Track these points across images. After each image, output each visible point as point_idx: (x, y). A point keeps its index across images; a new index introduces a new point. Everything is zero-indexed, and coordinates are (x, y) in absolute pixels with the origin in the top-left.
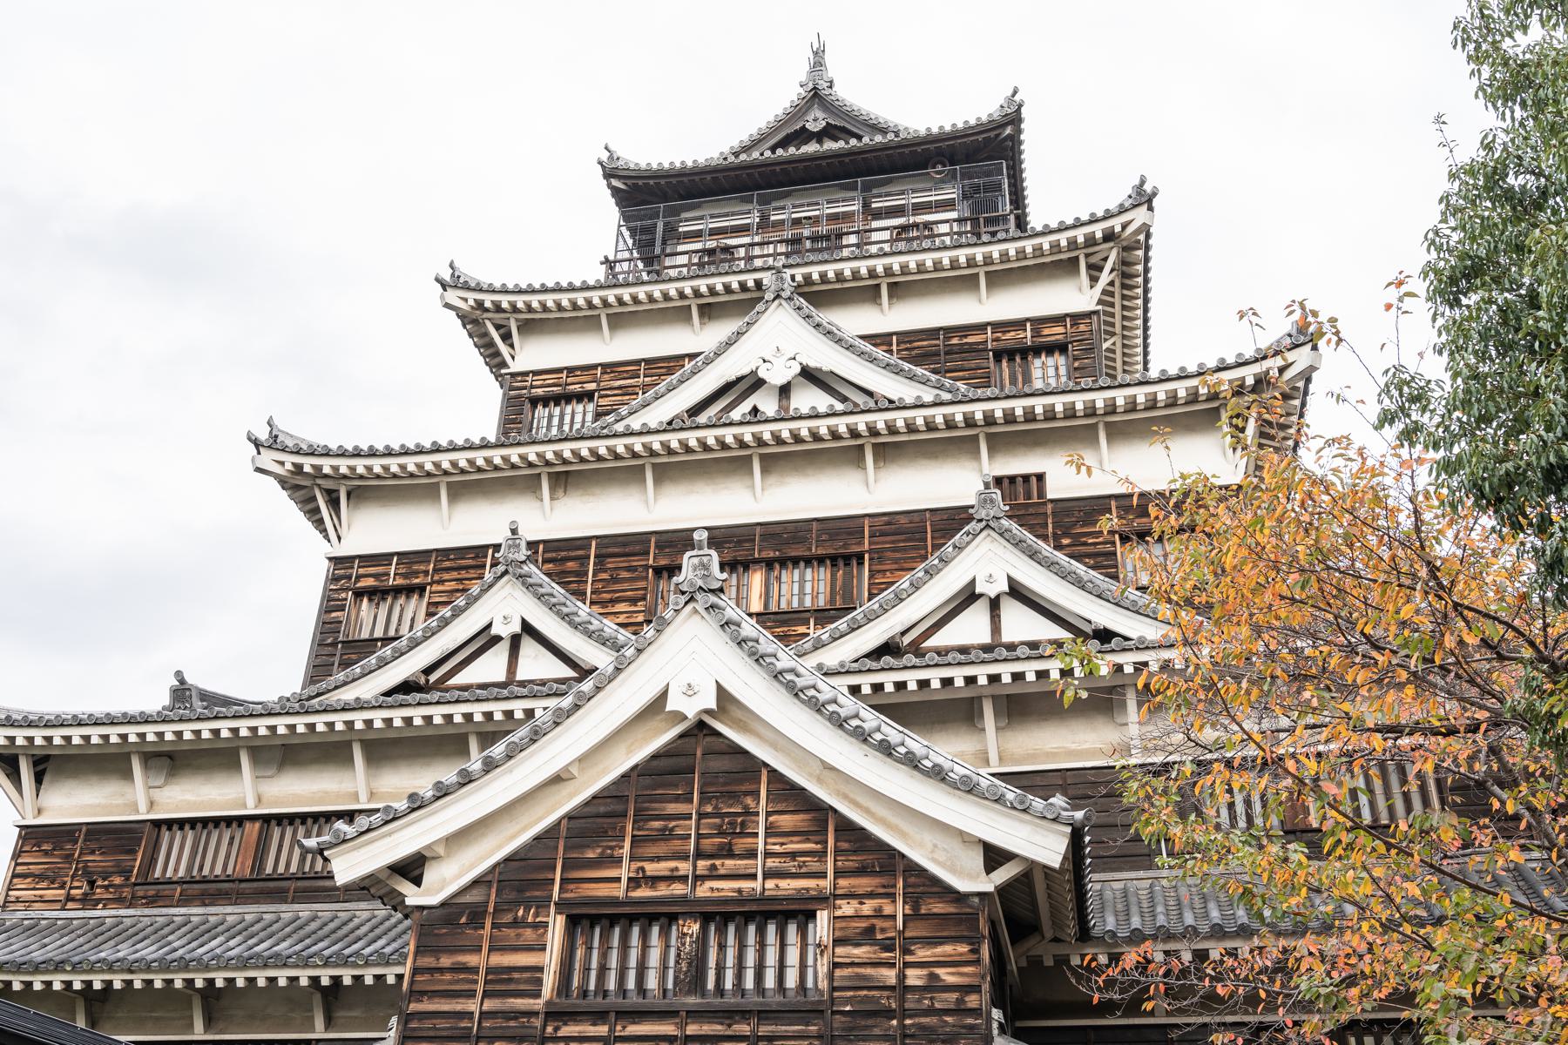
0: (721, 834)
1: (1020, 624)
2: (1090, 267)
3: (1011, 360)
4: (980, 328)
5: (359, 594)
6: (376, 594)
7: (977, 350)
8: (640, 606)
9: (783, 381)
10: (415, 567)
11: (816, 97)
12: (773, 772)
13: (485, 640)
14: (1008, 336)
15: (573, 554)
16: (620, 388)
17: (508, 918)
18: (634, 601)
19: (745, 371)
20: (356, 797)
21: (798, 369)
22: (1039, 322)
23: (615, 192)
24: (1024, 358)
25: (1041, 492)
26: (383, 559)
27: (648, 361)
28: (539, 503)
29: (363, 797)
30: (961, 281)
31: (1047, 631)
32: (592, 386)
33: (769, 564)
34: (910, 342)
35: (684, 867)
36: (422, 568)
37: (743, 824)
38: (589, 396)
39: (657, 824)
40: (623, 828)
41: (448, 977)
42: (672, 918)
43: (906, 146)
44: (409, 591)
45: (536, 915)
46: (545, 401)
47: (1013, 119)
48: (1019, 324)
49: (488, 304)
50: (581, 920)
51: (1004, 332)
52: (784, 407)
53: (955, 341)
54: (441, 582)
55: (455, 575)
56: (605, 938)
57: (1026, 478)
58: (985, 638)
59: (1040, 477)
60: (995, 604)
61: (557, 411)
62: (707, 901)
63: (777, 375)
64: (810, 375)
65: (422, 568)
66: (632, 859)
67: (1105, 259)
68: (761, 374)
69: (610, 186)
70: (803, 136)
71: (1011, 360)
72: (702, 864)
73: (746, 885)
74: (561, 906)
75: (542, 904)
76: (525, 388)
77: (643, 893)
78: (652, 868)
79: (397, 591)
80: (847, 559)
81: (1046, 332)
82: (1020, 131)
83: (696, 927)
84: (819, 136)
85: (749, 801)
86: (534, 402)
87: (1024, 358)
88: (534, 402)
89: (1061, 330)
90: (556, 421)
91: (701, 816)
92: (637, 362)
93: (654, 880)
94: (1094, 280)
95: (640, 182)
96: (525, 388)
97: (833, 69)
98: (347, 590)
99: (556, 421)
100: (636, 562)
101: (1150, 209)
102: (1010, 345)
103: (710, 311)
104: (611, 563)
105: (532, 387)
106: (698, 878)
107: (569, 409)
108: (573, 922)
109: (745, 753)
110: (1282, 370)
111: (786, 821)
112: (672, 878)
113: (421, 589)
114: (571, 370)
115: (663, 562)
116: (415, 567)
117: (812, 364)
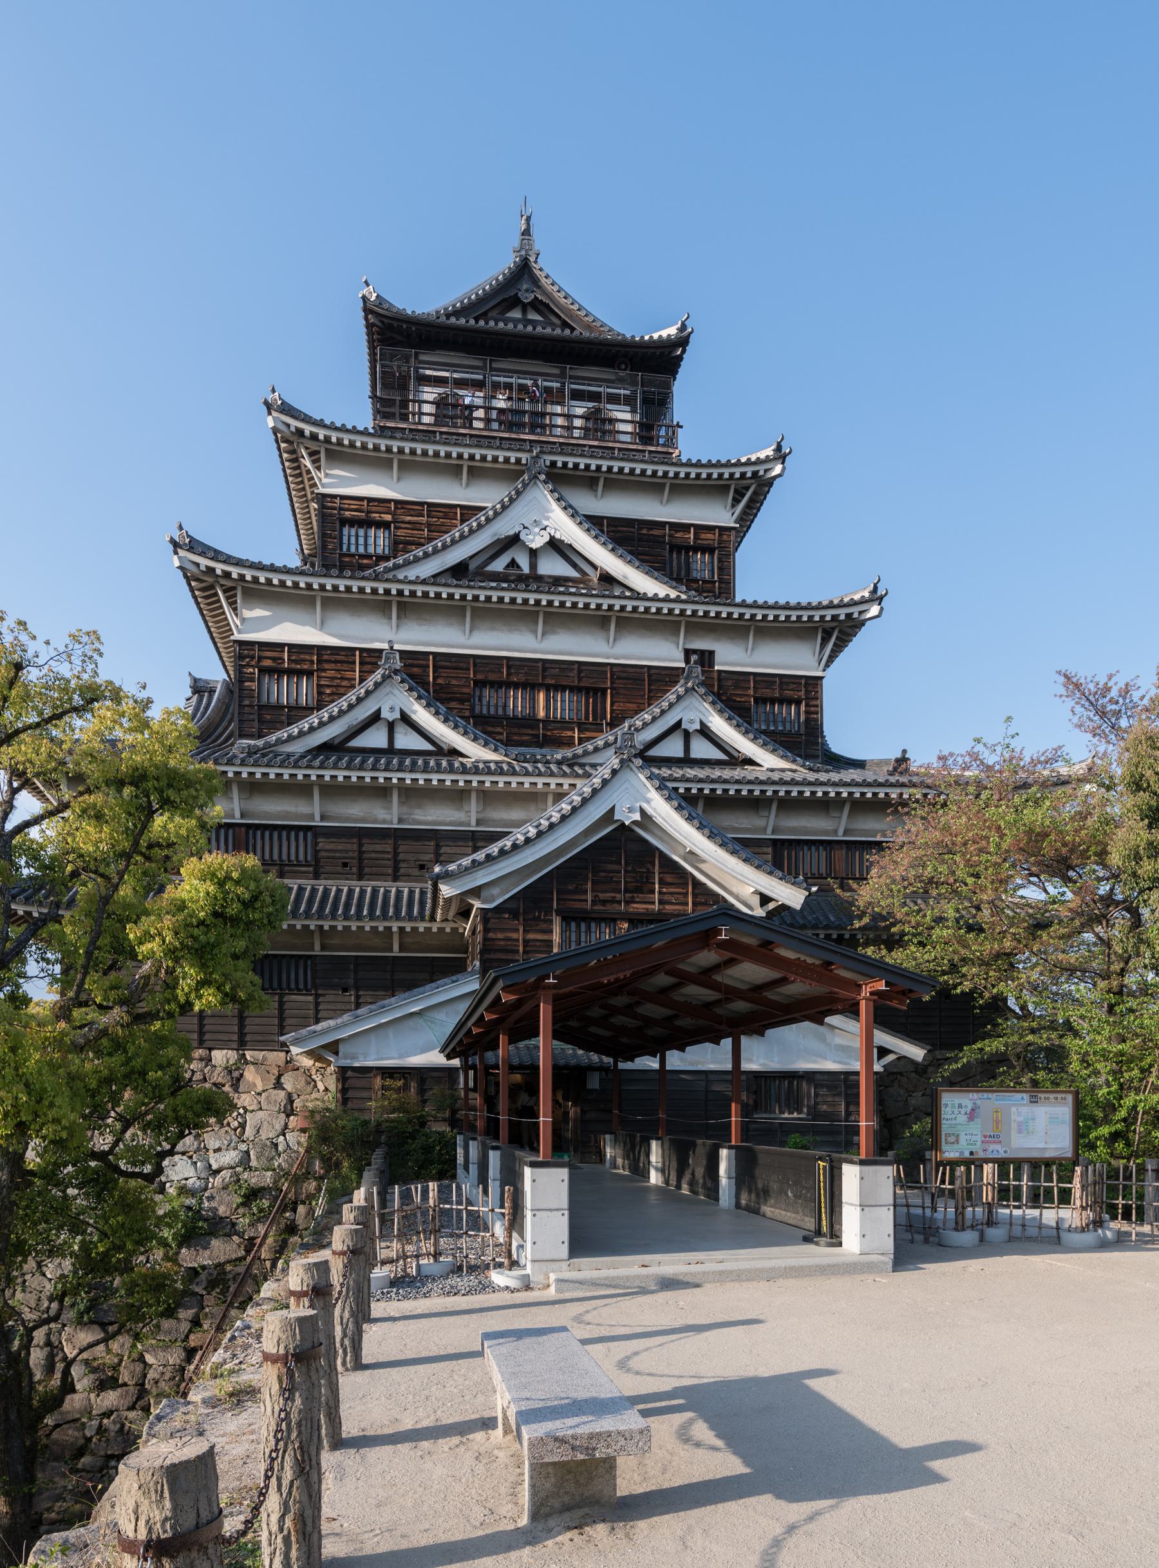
0: (637, 881)
1: (701, 749)
2: (736, 491)
3: (679, 553)
4: (662, 525)
5: (262, 671)
6: (278, 672)
7: (658, 541)
8: (467, 705)
9: (534, 546)
10: (302, 656)
11: (524, 270)
12: (661, 852)
13: (376, 717)
14: (678, 535)
15: (416, 662)
16: (409, 523)
17: (531, 916)
18: (461, 701)
19: (511, 533)
20: (311, 817)
21: (547, 538)
22: (700, 528)
23: (369, 326)
24: (687, 553)
25: (711, 665)
26: (279, 646)
27: (430, 505)
28: (386, 621)
29: (318, 818)
30: (652, 486)
31: (717, 754)
32: (388, 517)
33: (548, 688)
34: (616, 526)
35: (618, 896)
36: (307, 657)
37: (647, 878)
38: (385, 525)
39: (603, 874)
40: (587, 876)
41: (502, 943)
42: (614, 920)
43: (604, 345)
44: (300, 673)
45: (545, 915)
46: (352, 522)
47: (682, 341)
48: (685, 527)
49: (307, 433)
50: (566, 919)
51: (677, 532)
52: (533, 566)
53: (644, 531)
54: (324, 670)
55: (332, 666)
56: (578, 927)
57: (702, 653)
58: (680, 754)
59: (712, 653)
60: (687, 735)
61: (361, 532)
62: (632, 913)
63: (537, 541)
64: (556, 546)
65: (307, 657)
66: (593, 891)
67: (747, 488)
68: (522, 536)
69: (366, 319)
70: (515, 302)
71: (679, 553)
72: (628, 895)
73: (650, 906)
74: (558, 913)
75: (549, 911)
76: (334, 508)
77: (598, 907)
78: (602, 896)
79: (290, 672)
80: (595, 691)
81: (703, 536)
82: (684, 352)
83: (626, 925)
84: (525, 308)
85: (649, 866)
86: (344, 522)
87: (687, 553)
88: (344, 522)
89: (710, 536)
90: (361, 541)
91: (626, 872)
92: (422, 504)
93: (604, 902)
94: (736, 501)
95: (395, 324)
96: (334, 508)
97: (539, 242)
98: (252, 666)
99: (361, 541)
100: (461, 673)
101: (783, 463)
102: (678, 542)
103: (478, 472)
104: (444, 673)
105: (341, 509)
106: (627, 903)
107: (372, 532)
108: (564, 919)
109: (646, 842)
110: (861, 613)
111: (669, 878)
112: (613, 901)
113: (309, 674)
114: (370, 500)
115: (480, 677)
116: (302, 656)
117: (558, 536)
